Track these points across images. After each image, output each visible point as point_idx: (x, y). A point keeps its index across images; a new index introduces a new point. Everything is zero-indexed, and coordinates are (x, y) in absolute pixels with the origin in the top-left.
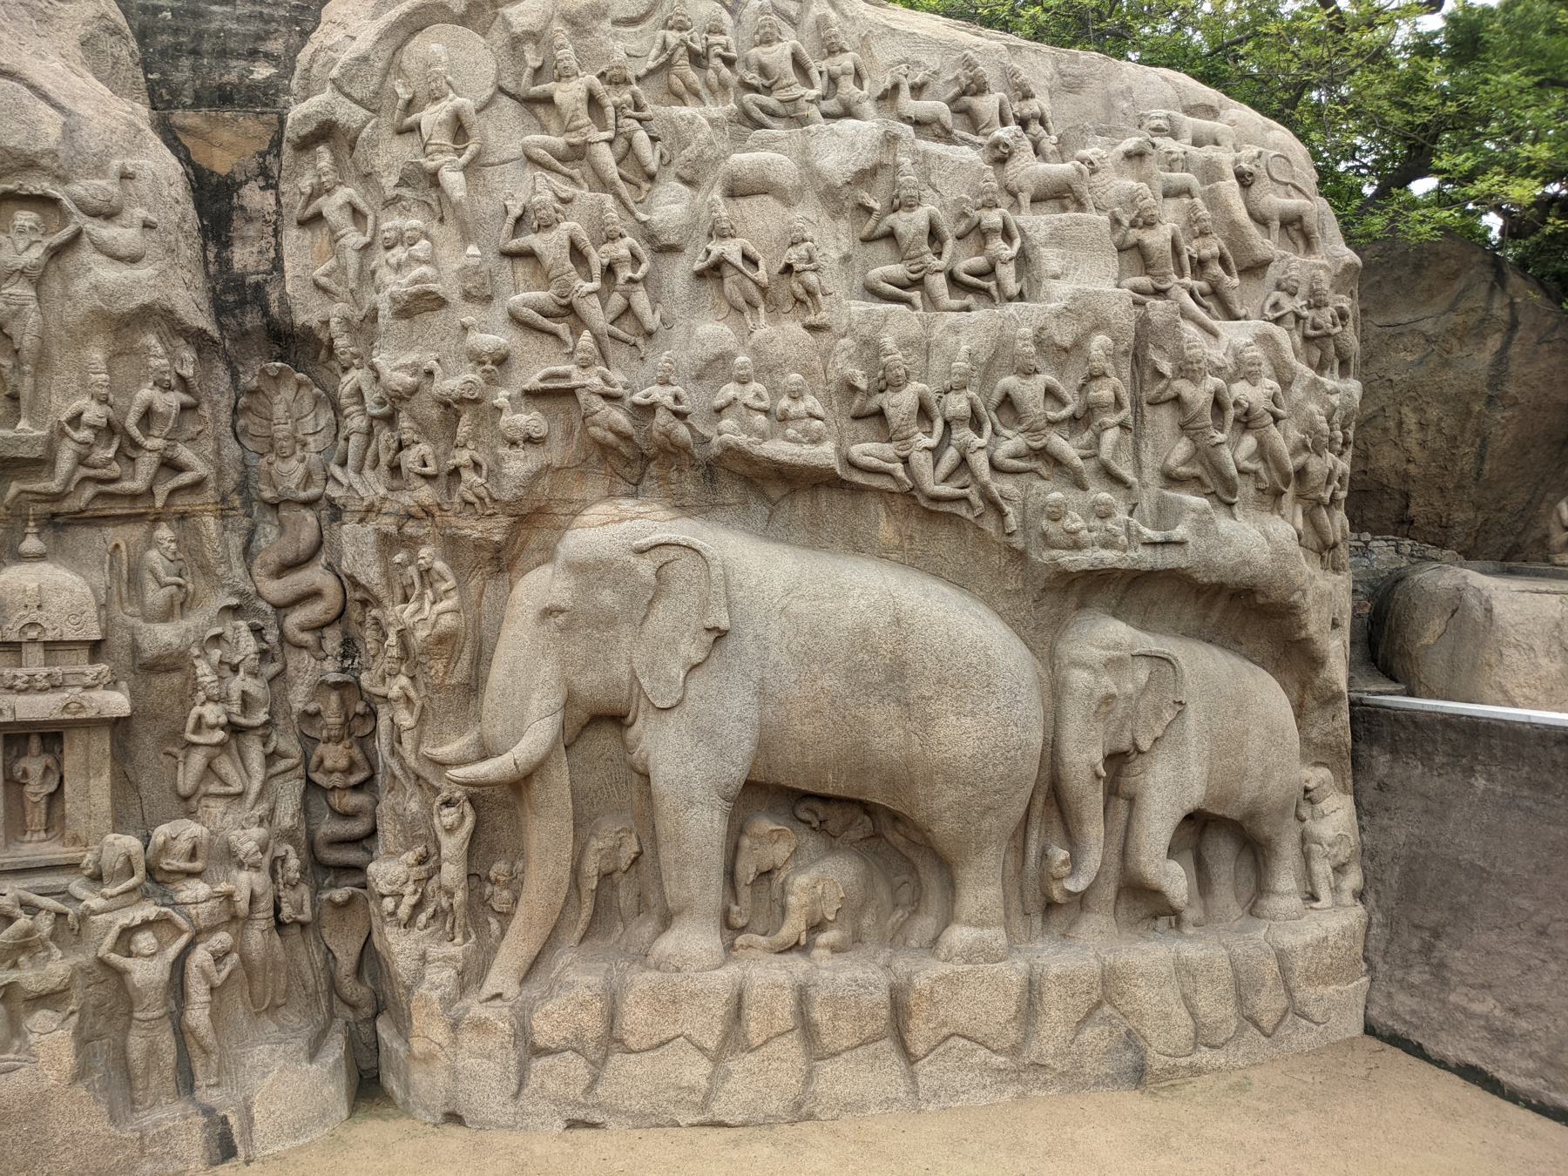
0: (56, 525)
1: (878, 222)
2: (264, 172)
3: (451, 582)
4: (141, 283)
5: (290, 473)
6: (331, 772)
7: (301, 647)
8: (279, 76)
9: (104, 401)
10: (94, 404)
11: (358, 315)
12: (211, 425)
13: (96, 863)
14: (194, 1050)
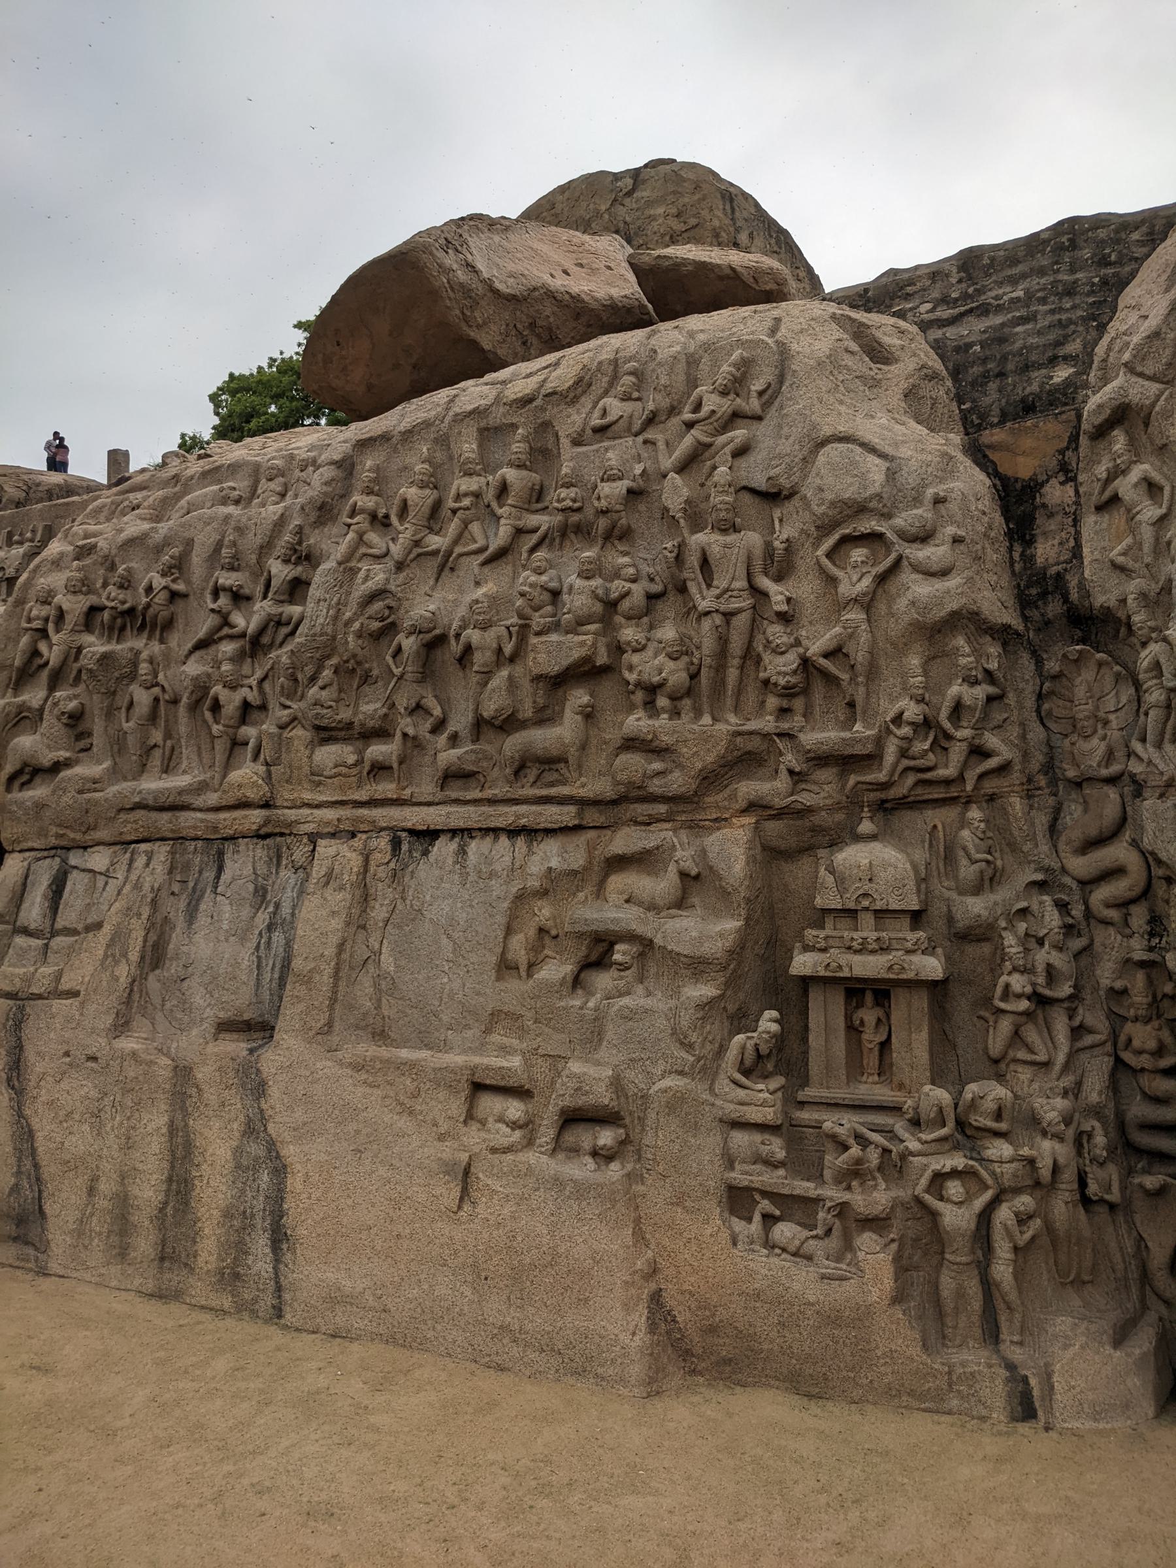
0: (886, 810)
2: (1064, 468)
4: (949, 594)
5: (1092, 751)
6: (1140, 1052)
7: (1107, 923)
8: (1077, 374)
9: (921, 700)
10: (912, 703)
11: (1155, 587)
12: (1016, 712)
13: (916, 1109)
14: (1000, 1305)
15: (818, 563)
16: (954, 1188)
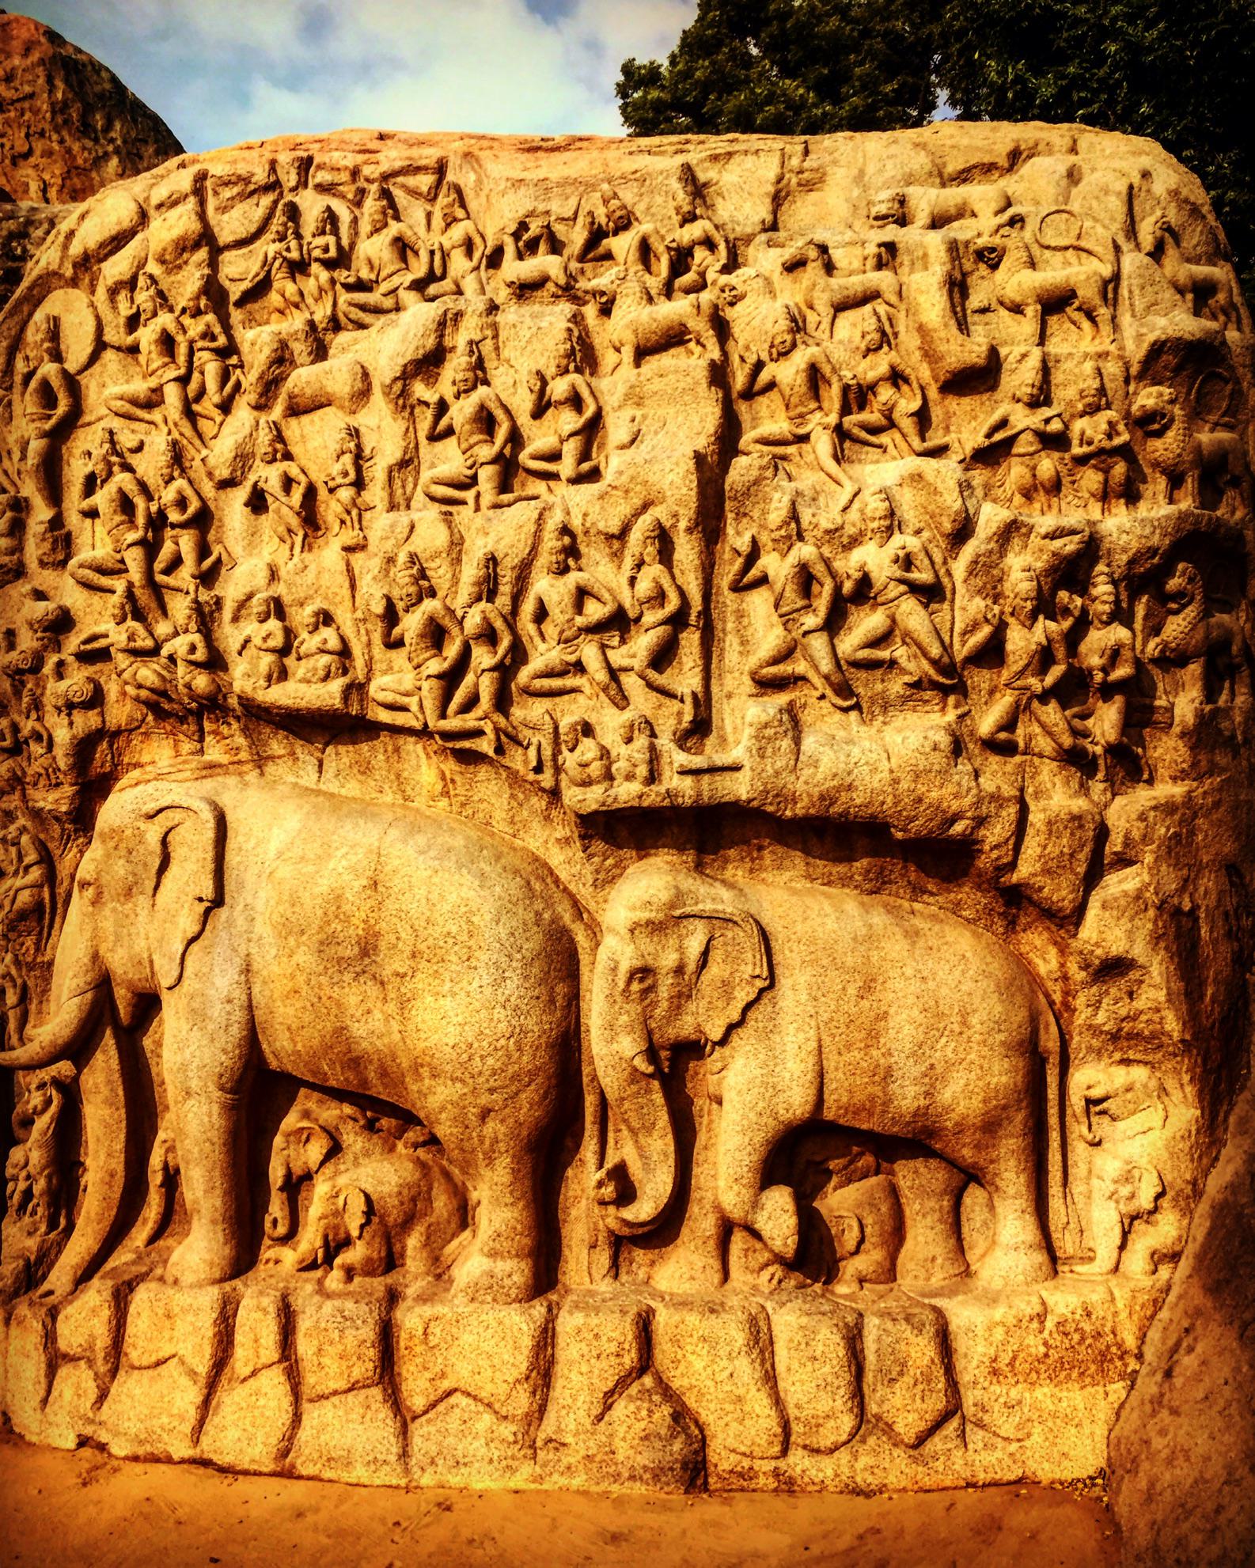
1: (438, 417)
3: (31, 857)
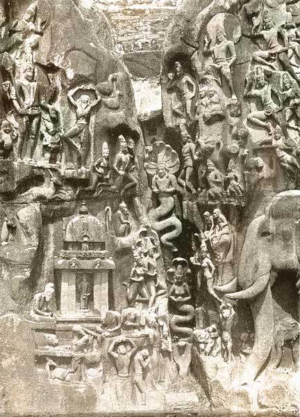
3: (226, 223)
9: (107, 159)
15: (69, 99)
16: (122, 348)
